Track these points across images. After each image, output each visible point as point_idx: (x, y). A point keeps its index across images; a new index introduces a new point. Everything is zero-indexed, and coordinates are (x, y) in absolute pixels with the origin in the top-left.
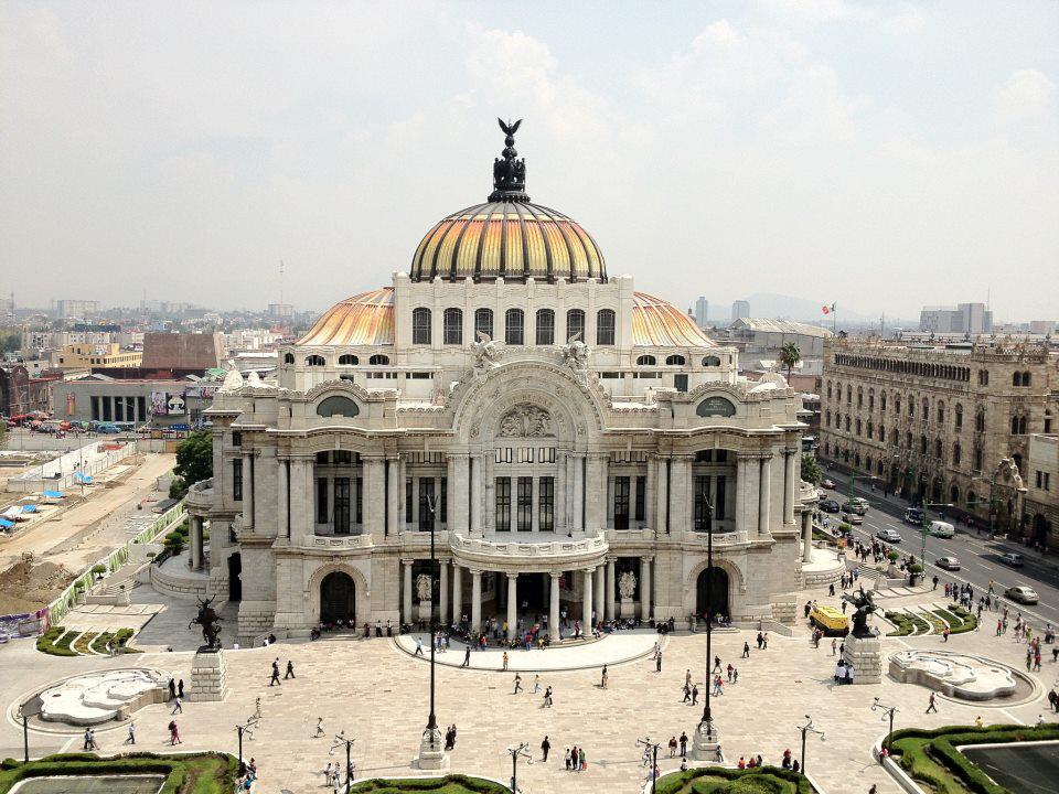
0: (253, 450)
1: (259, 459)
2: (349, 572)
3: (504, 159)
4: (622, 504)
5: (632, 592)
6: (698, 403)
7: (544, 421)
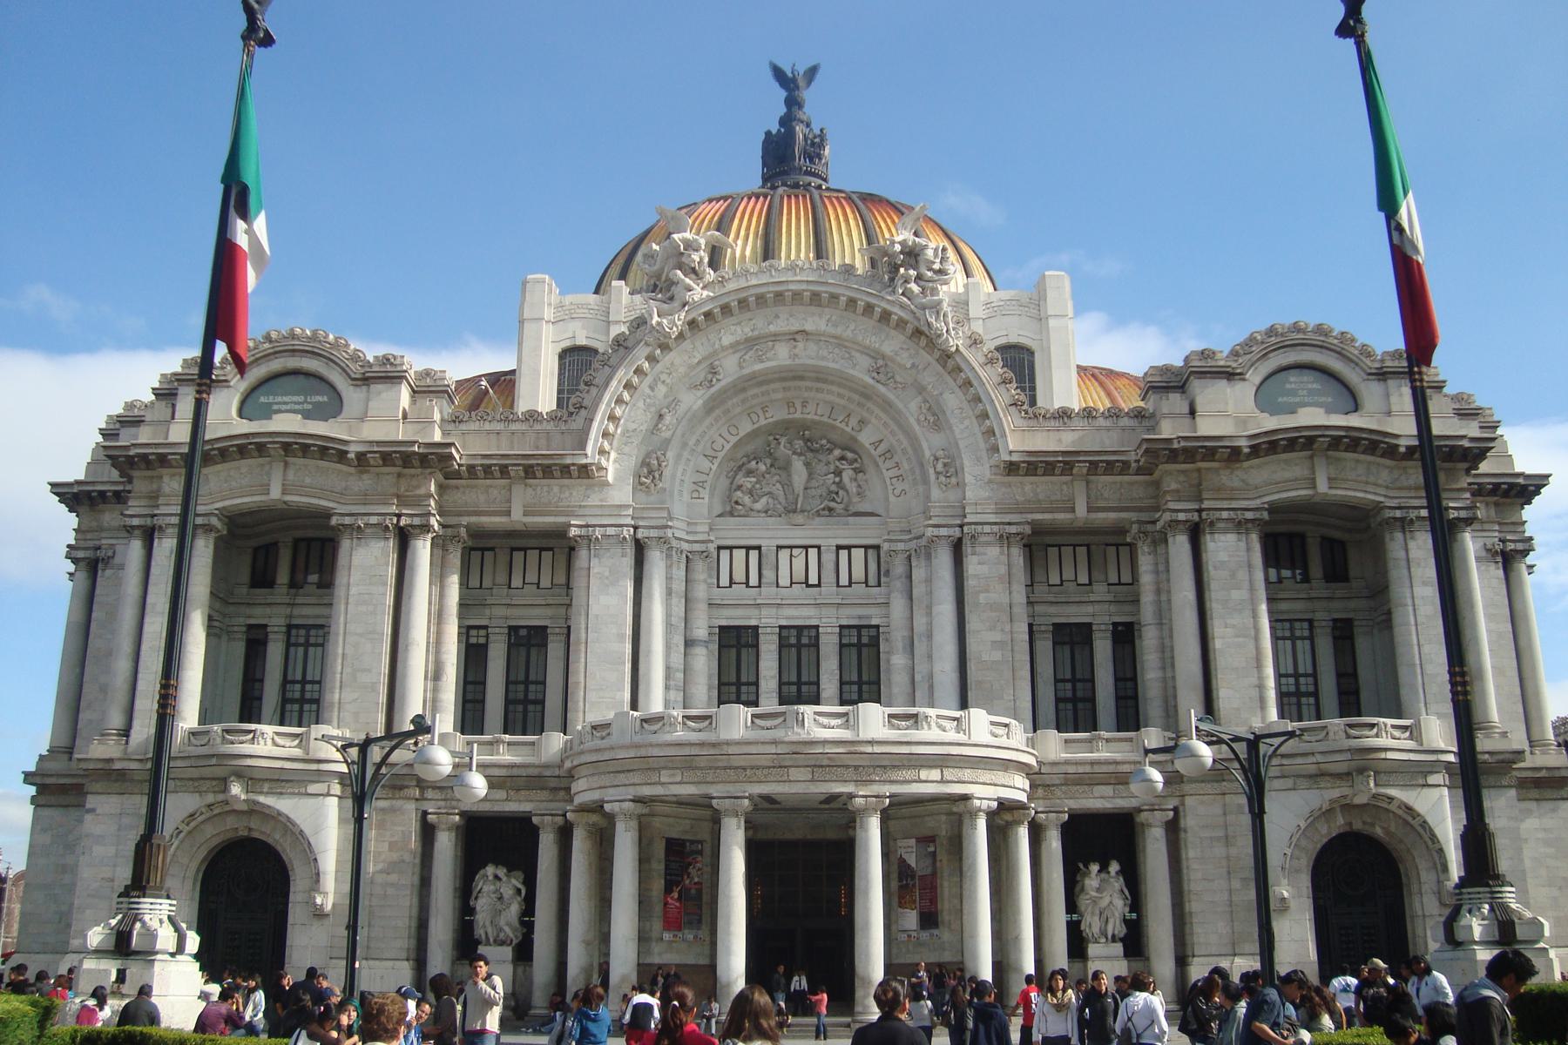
1: (108, 572)
2: (275, 838)
4: (1074, 700)
5: (1116, 927)
6: (1255, 377)
7: (847, 475)
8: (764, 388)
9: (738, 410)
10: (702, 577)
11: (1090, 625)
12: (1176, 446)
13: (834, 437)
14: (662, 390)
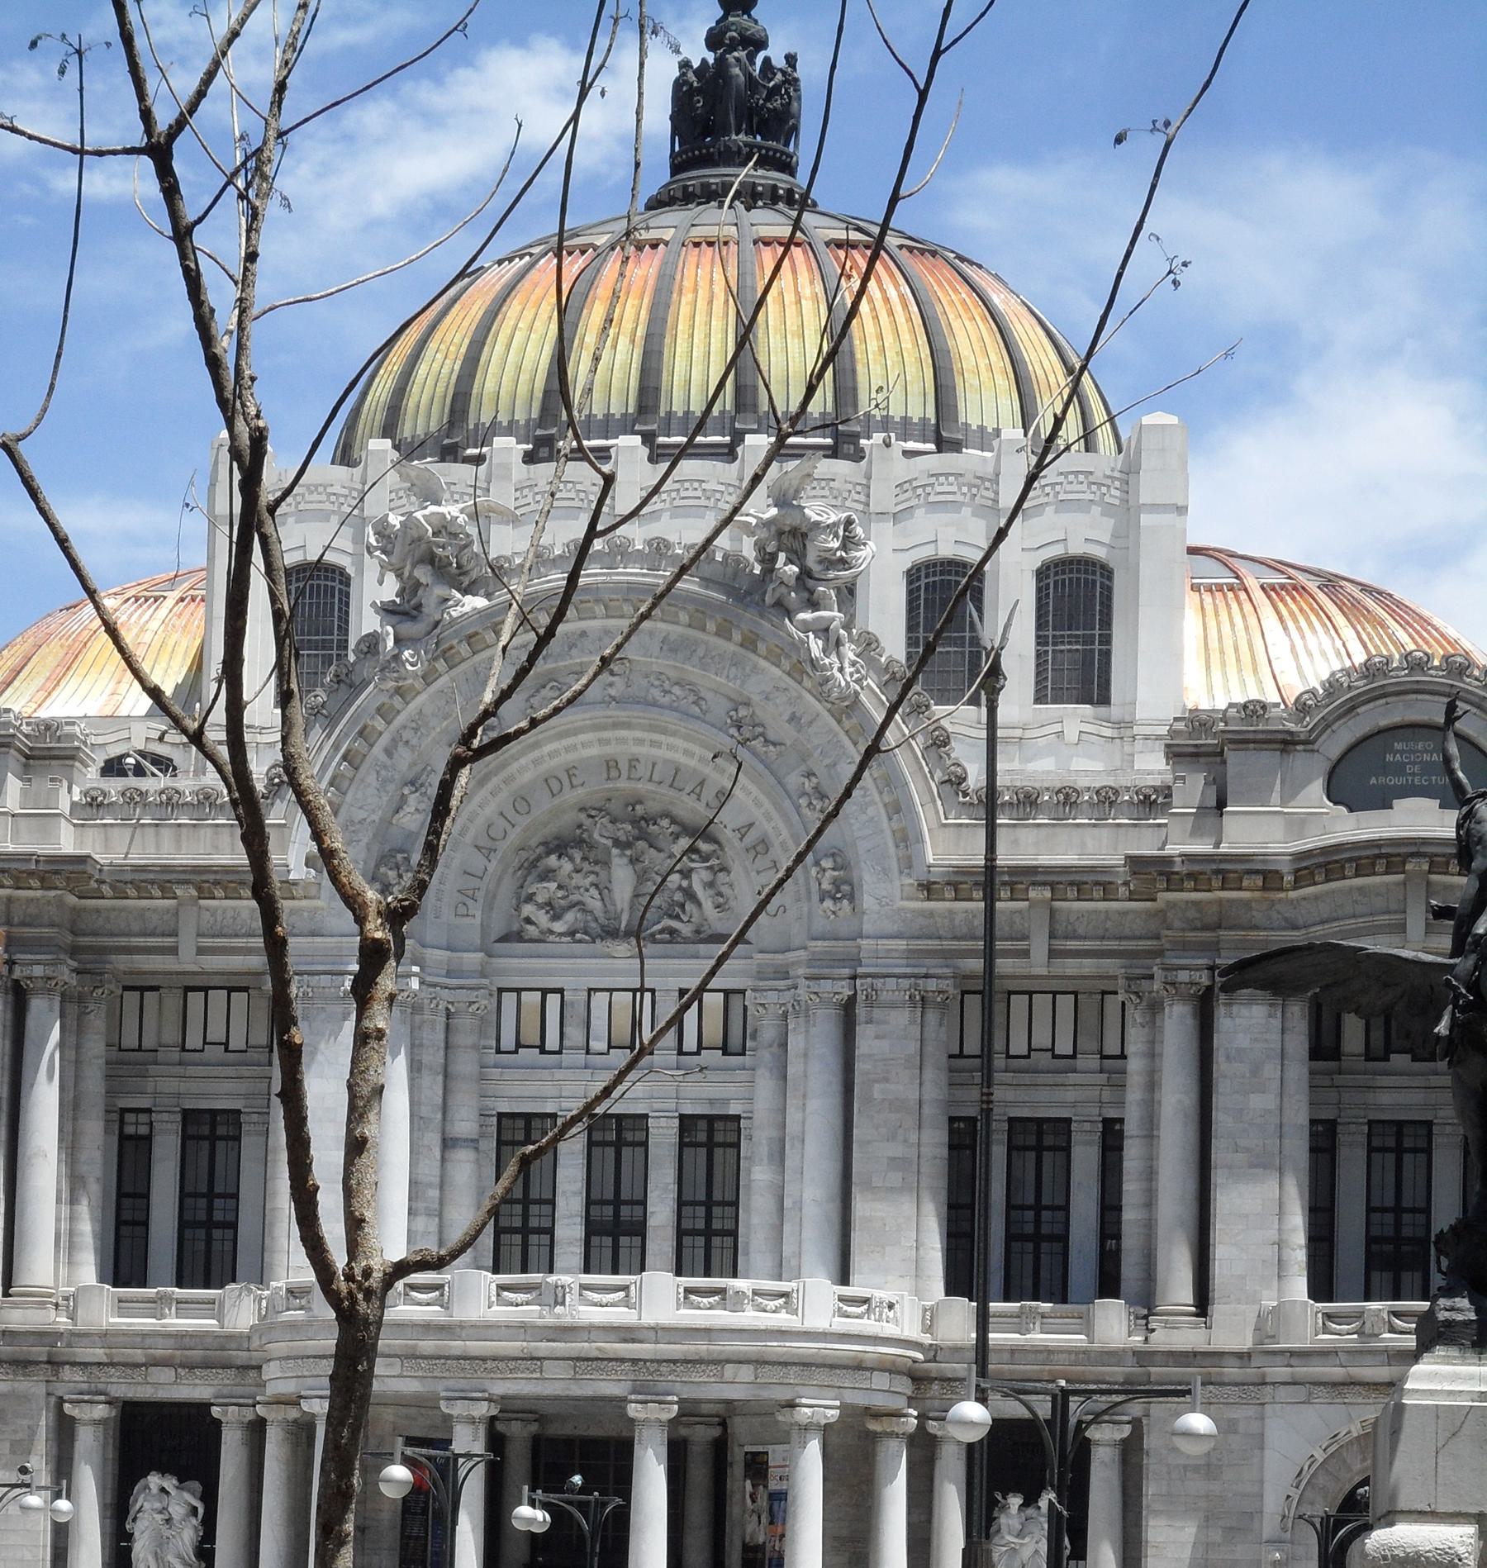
3: (711, 58)
4: (1037, 1238)
8: (566, 742)
9: (527, 777)
10: (471, 1040)
11: (1068, 1121)
13: (681, 813)
14: (404, 757)
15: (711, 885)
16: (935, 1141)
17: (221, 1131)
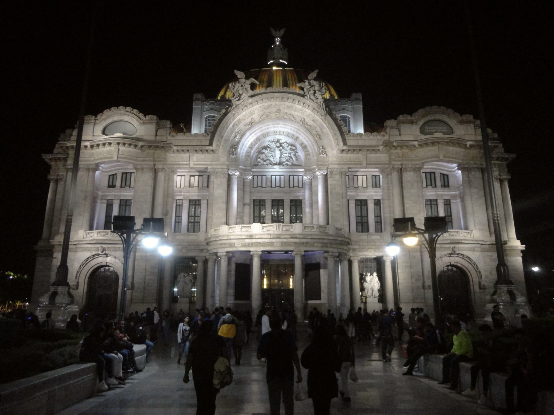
0: (58, 175)
4: (362, 223)
11: (366, 200)
12: (395, 144)
13: (288, 142)
15: (295, 155)
16: (345, 201)
17: (197, 204)
